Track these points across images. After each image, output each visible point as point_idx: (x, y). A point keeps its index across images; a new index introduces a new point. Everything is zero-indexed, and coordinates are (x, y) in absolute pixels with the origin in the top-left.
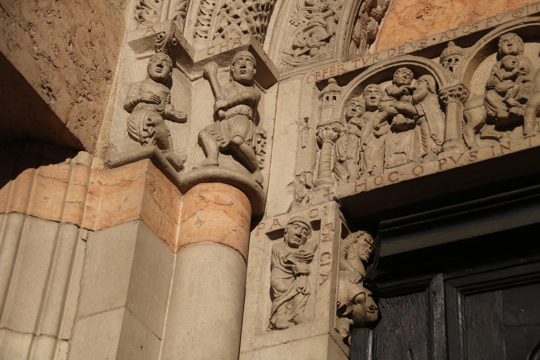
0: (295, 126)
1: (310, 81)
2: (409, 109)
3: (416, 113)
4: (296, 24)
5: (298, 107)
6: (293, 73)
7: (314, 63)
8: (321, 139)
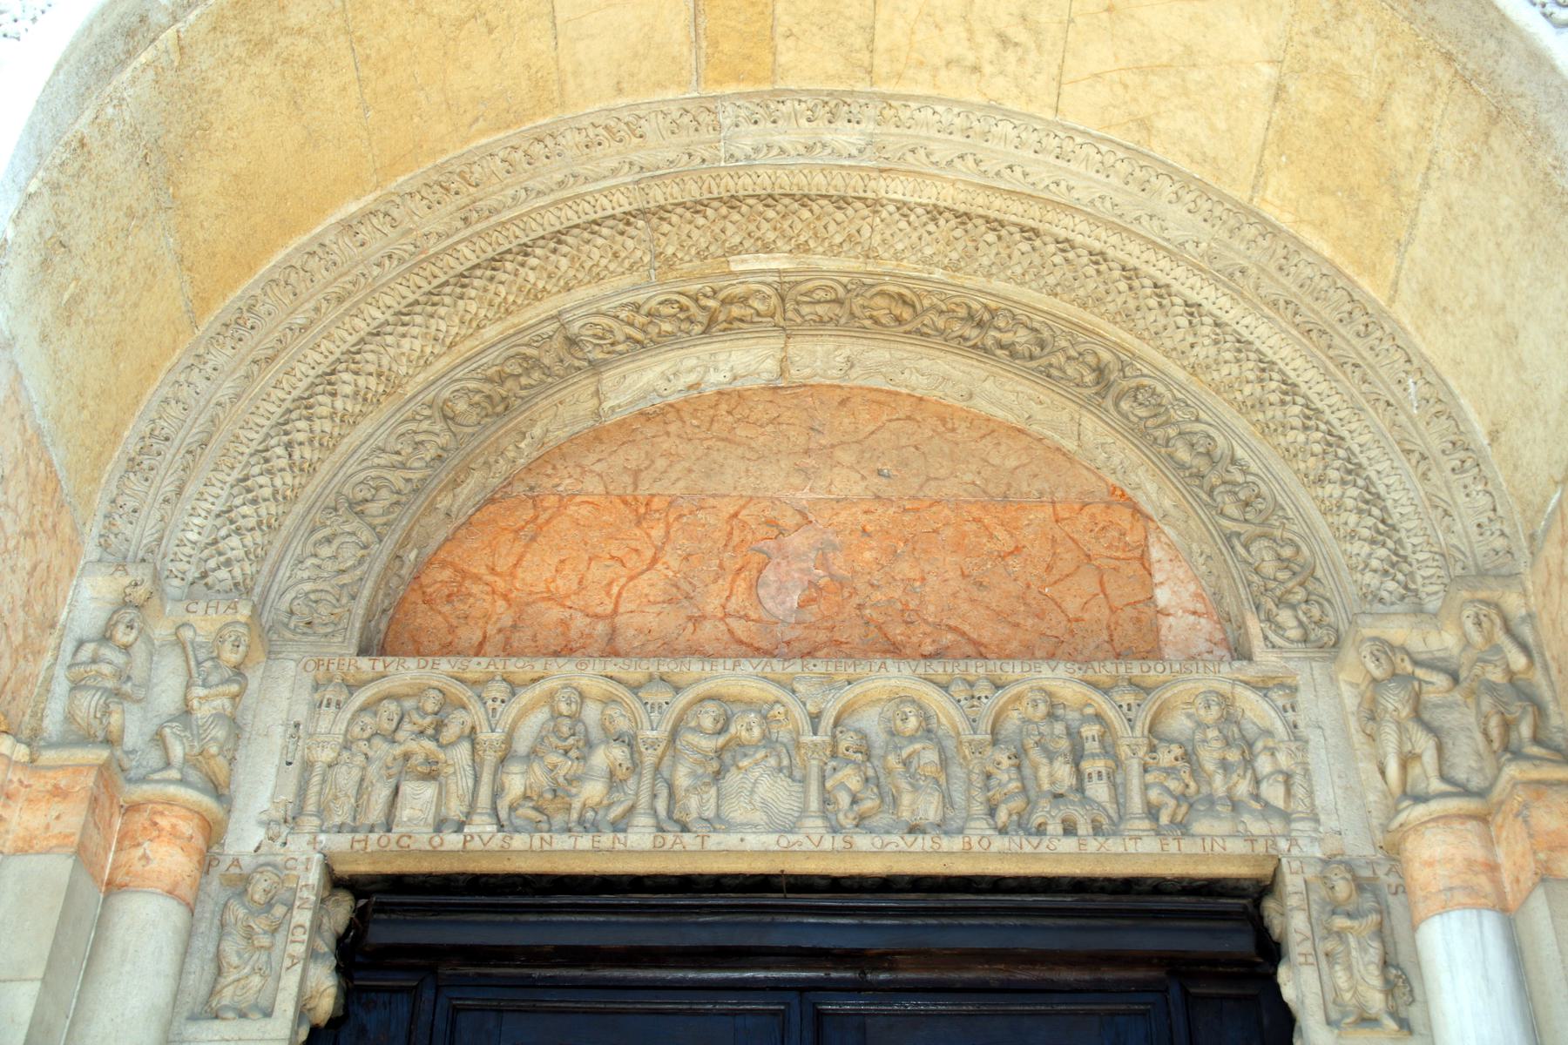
0: (280, 729)
1: (309, 669)
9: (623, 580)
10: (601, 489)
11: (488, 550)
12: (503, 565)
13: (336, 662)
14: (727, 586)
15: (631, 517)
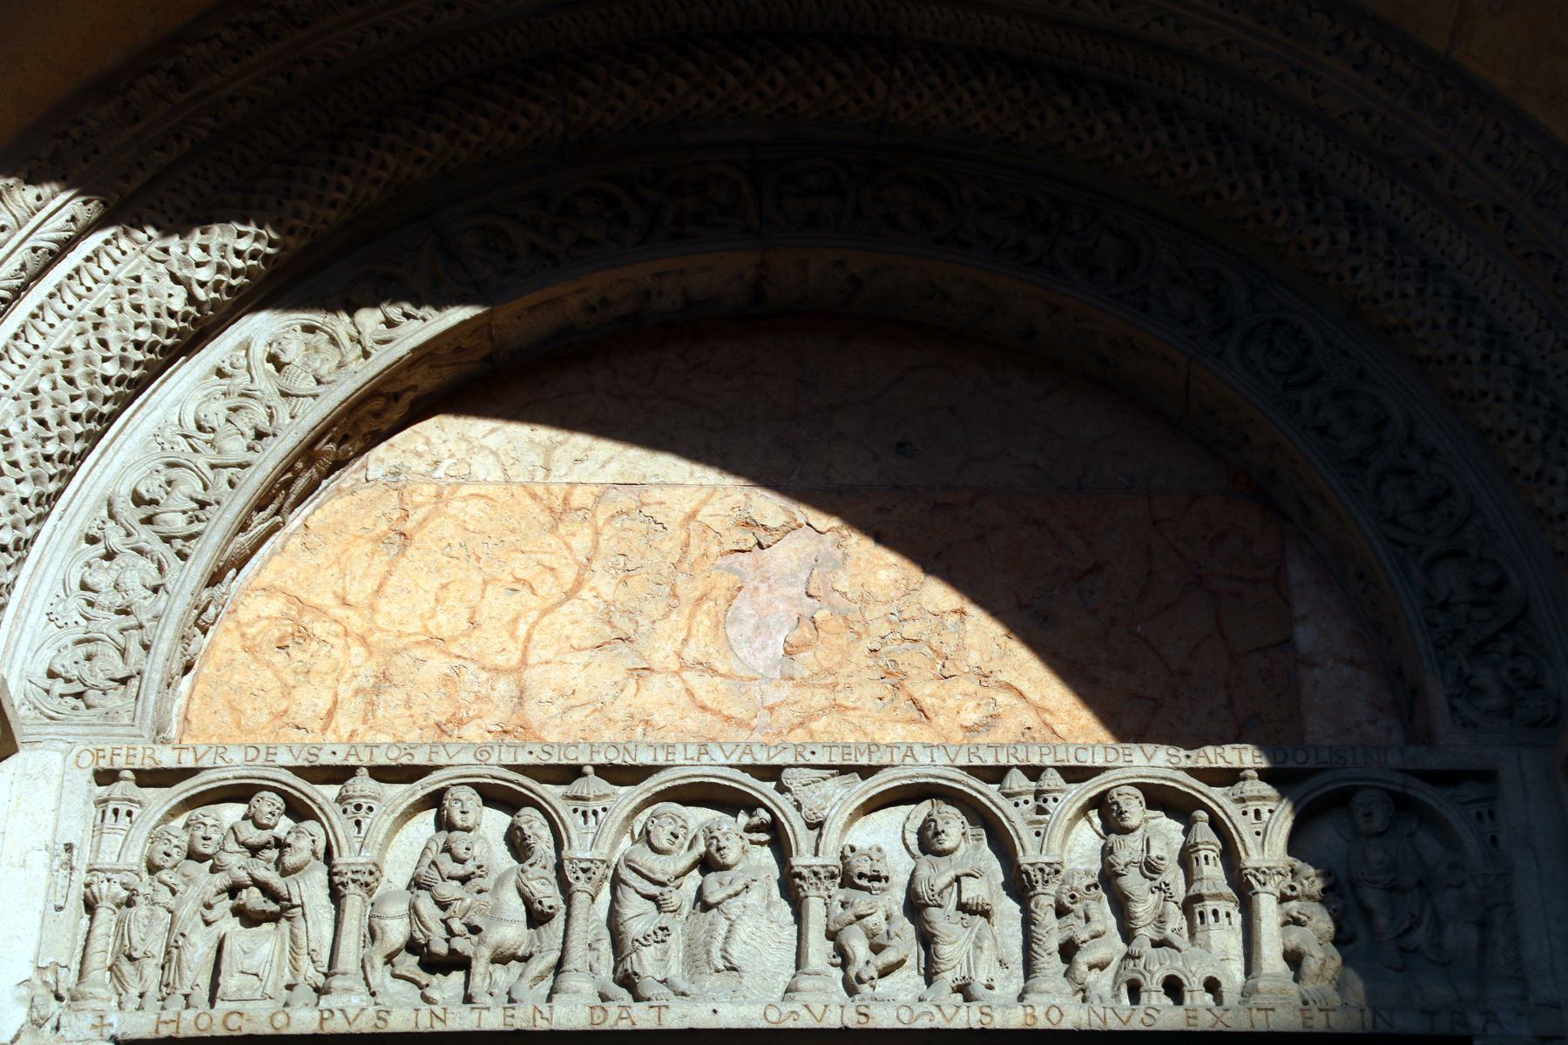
0: (44, 857)
2: (275, 885)
3: (287, 896)
4: (60, 623)
5: (52, 813)
6: (48, 734)
7: (94, 725)
8: (95, 897)
9: (534, 615)
10: (497, 475)
11: (335, 570)
12: (359, 591)
13: (124, 752)
14: (683, 623)
15: (545, 518)
